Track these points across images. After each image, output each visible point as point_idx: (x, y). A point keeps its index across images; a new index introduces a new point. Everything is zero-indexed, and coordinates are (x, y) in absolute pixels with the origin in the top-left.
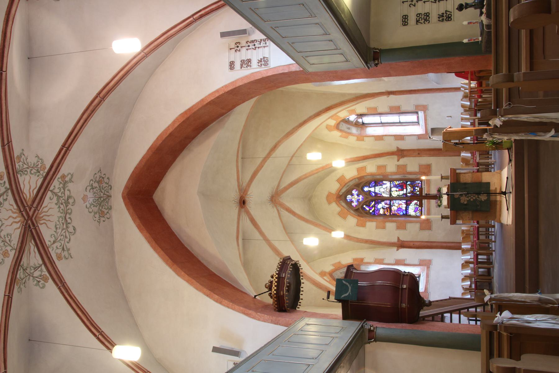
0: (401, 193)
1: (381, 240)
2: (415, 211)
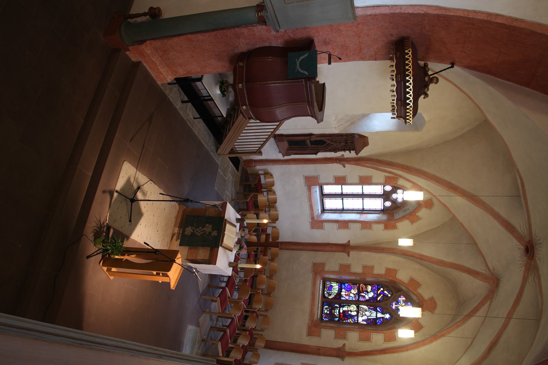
0: (345, 309)
1: (368, 253)
2: (332, 286)
